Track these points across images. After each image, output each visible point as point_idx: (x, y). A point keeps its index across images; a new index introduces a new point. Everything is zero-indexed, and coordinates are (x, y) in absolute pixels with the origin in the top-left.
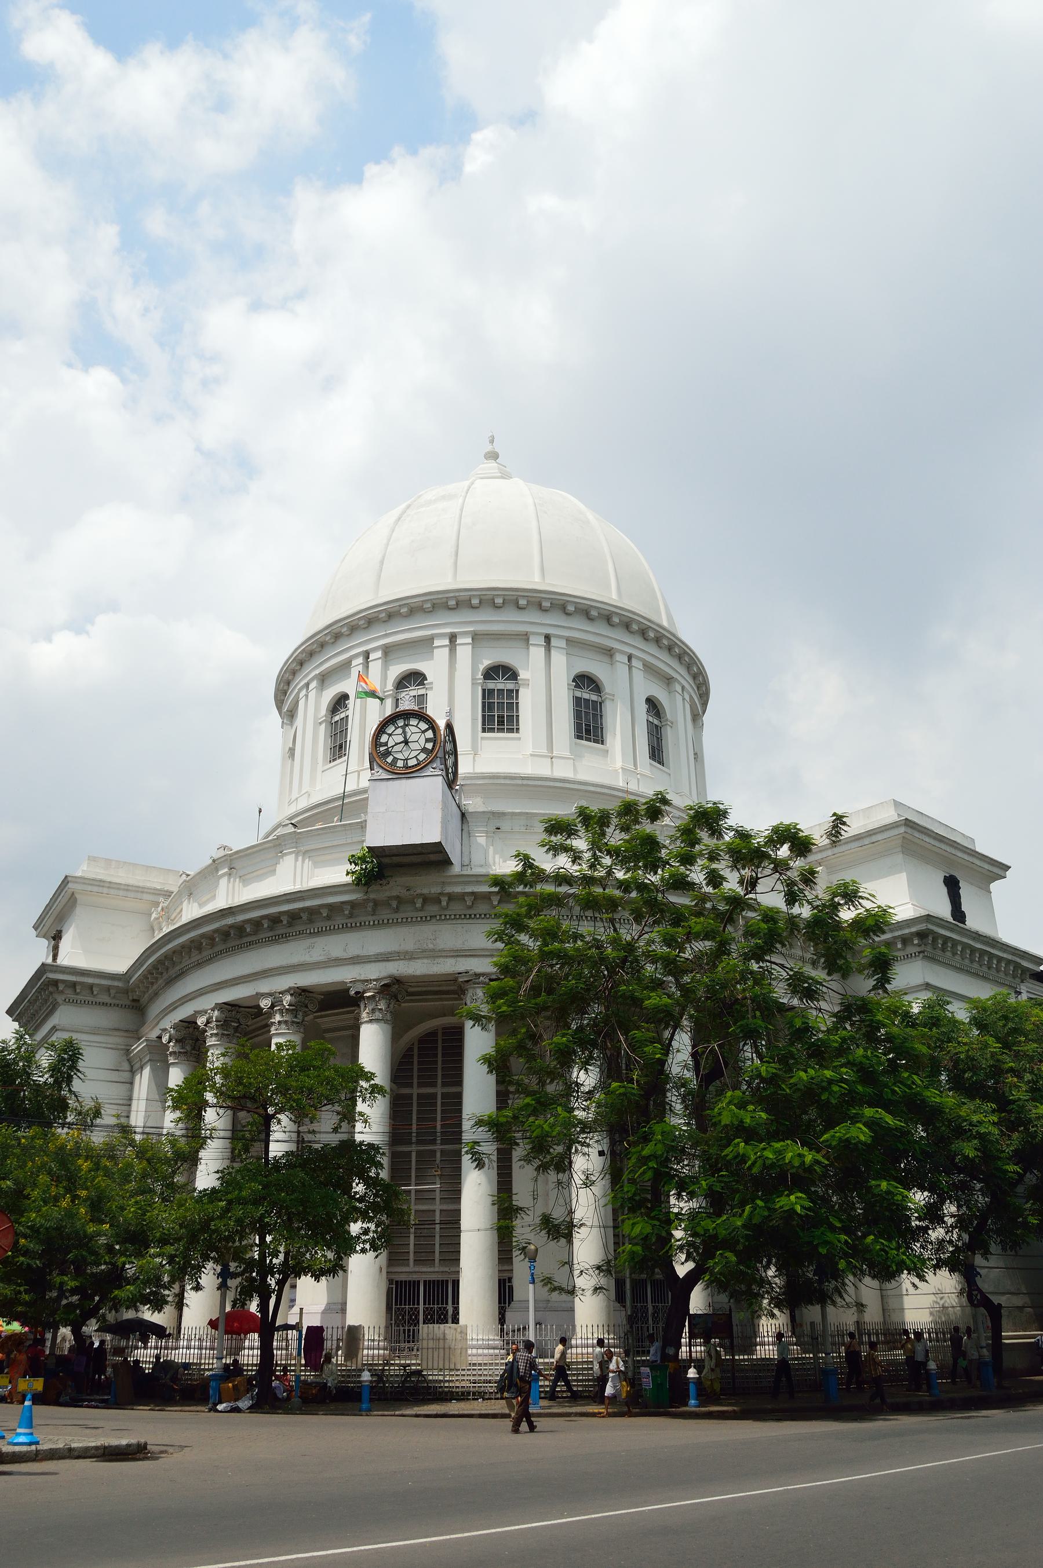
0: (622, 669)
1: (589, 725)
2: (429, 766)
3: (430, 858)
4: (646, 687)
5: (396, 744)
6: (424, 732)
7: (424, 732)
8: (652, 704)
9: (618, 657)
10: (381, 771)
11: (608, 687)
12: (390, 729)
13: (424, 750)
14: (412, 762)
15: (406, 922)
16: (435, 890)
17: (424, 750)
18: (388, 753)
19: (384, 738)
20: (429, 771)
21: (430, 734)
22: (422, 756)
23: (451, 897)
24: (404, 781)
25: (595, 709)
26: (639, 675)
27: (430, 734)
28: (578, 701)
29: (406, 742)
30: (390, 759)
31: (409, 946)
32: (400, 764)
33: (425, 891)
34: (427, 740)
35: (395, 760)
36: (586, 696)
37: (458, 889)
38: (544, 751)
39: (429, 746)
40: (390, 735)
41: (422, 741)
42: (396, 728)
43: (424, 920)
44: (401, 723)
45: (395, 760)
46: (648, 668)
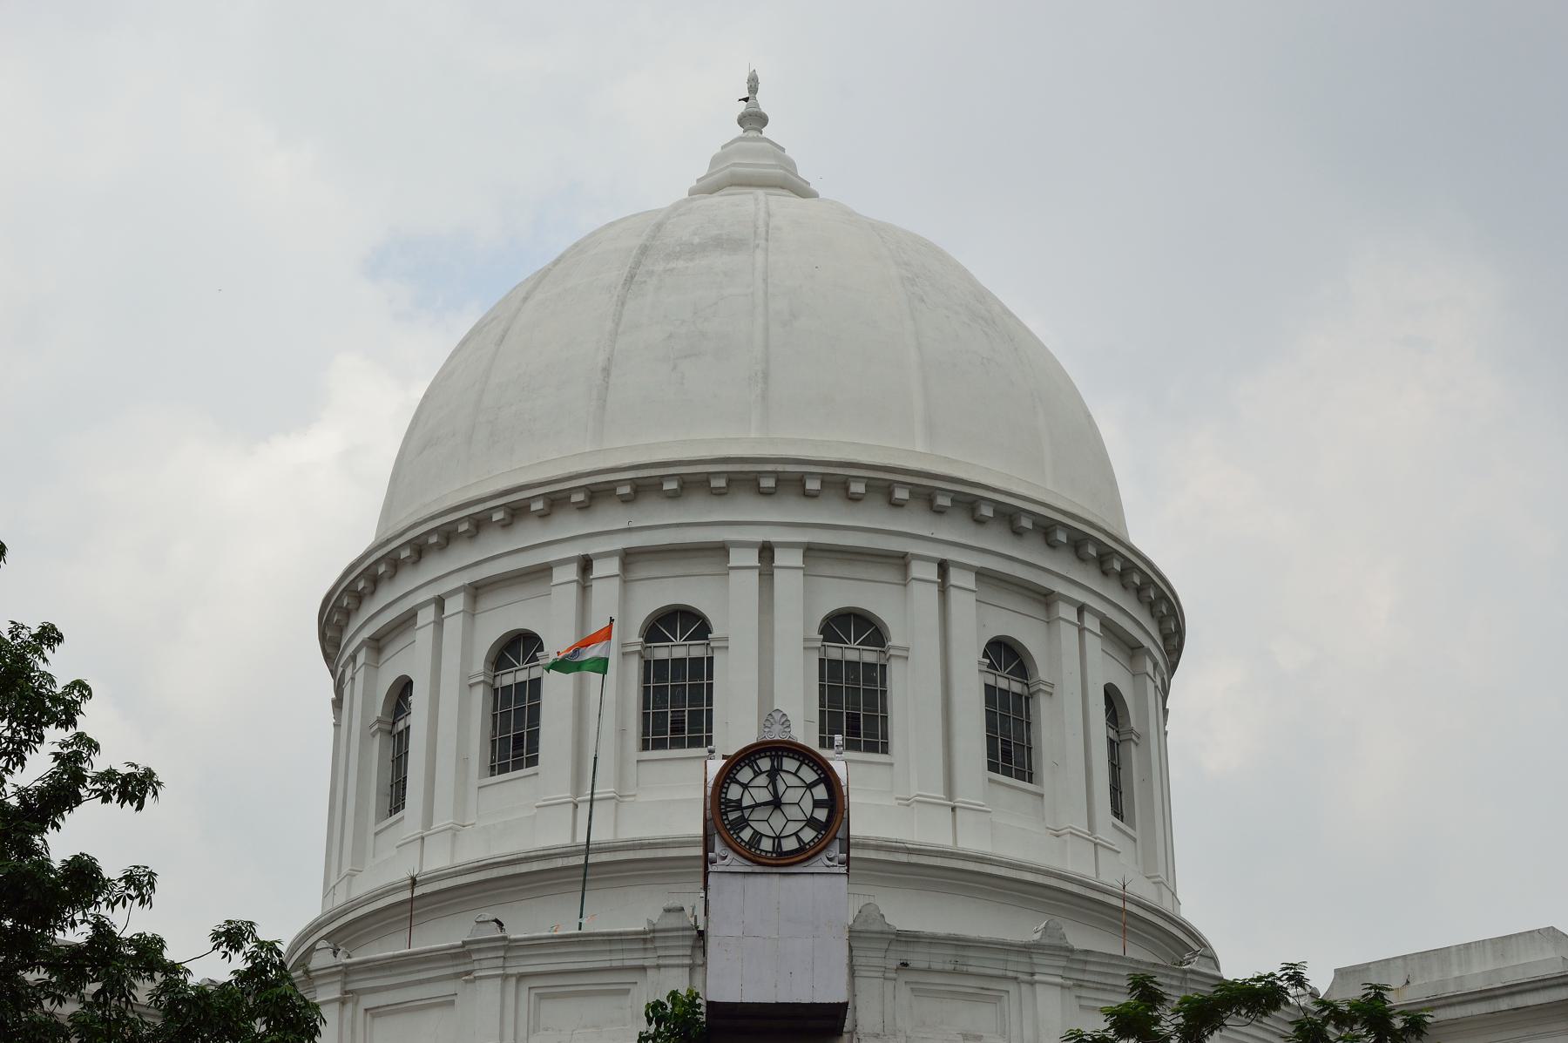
0: (1069, 635)
2: (823, 856)
4: (1105, 668)
5: (758, 805)
6: (810, 786)
7: (810, 786)
8: (1112, 697)
9: (1067, 612)
10: (731, 855)
11: (1043, 670)
13: (811, 822)
14: (790, 845)
17: (811, 822)
18: (743, 823)
19: (734, 792)
21: (821, 792)
22: (808, 835)
24: (776, 878)
25: (1018, 711)
26: (1094, 645)
28: (990, 690)
29: (776, 803)
30: (746, 834)
32: (766, 845)
34: (817, 804)
35: (758, 836)
36: (1003, 684)
38: (939, 793)
39: (822, 815)
40: (745, 787)
41: (807, 805)
42: (757, 774)
44: (765, 764)
45: (758, 836)
46: (1108, 628)
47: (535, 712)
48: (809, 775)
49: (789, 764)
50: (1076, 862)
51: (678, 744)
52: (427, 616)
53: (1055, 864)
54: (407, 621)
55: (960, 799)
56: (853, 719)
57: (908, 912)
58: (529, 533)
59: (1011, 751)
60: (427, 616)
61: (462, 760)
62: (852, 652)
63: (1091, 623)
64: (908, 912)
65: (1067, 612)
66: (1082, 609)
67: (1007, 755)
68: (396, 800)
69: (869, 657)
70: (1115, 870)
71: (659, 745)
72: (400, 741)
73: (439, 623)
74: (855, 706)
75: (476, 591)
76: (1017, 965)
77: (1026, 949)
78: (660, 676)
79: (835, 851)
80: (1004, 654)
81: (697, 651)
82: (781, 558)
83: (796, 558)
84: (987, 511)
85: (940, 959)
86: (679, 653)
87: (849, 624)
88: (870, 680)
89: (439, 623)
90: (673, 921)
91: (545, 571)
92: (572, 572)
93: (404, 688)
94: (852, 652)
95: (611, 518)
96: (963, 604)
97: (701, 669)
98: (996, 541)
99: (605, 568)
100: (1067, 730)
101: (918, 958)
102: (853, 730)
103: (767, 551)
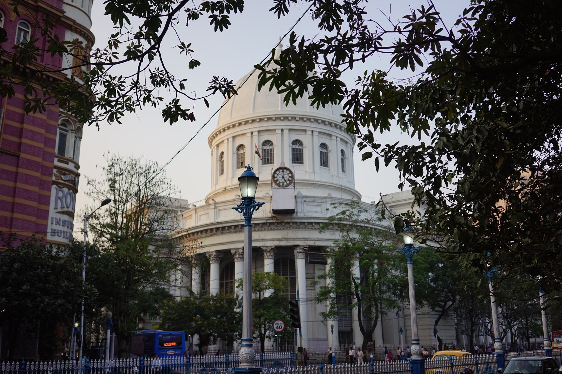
1: (324, 162)
3: (291, 212)
12: (278, 172)
15: (278, 229)
16: (289, 221)
19: (276, 175)
20: (290, 187)
23: (293, 223)
27: (290, 175)
31: (280, 237)
32: (281, 184)
33: (286, 221)
35: (280, 183)
37: (296, 221)
38: (312, 171)
41: (288, 177)
43: (284, 229)
44: (281, 170)
45: (280, 183)
47: (244, 157)
48: (288, 172)
49: (285, 170)
50: (335, 181)
51: (268, 163)
52: (226, 141)
53: (332, 182)
54: (223, 141)
55: (315, 171)
56: (297, 158)
57: (305, 192)
58: (243, 127)
59: (324, 162)
60: (226, 141)
61: (233, 166)
62: (297, 147)
63: (338, 139)
64: (305, 192)
65: (334, 138)
66: (337, 137)
67: (324, 163)
68: (222, 172)
69: (300, 147)
70: (343, 182)
71: (265, 164)
72: (222, 162)
73: (228, 143)
74: (297, 157)
75: (234, 137)
76: (324, 200)
77: (325, 198)
78: (265, 152)
79: (292, 184)
80: (323, 145)
81: (271, 148)
82: (285, 131)
83: (287, 131)
84: (320, 121)
85: (311, 200)
86: (268, 148)
87: (297, 142)
88: (300, 151)
89: (228, 143)
90: (267, 195)
91: (245, 134)
92: (250, 134)
93: (222, 153)
94: (297, 147)
95: (256, 125)
96: (316, 138)
97: (272, 151)
98: (322, 126)
99: (255, 134)
100: (334, 158)
101: (307, 200)
102: (297, 160)
103: (282, 130)
